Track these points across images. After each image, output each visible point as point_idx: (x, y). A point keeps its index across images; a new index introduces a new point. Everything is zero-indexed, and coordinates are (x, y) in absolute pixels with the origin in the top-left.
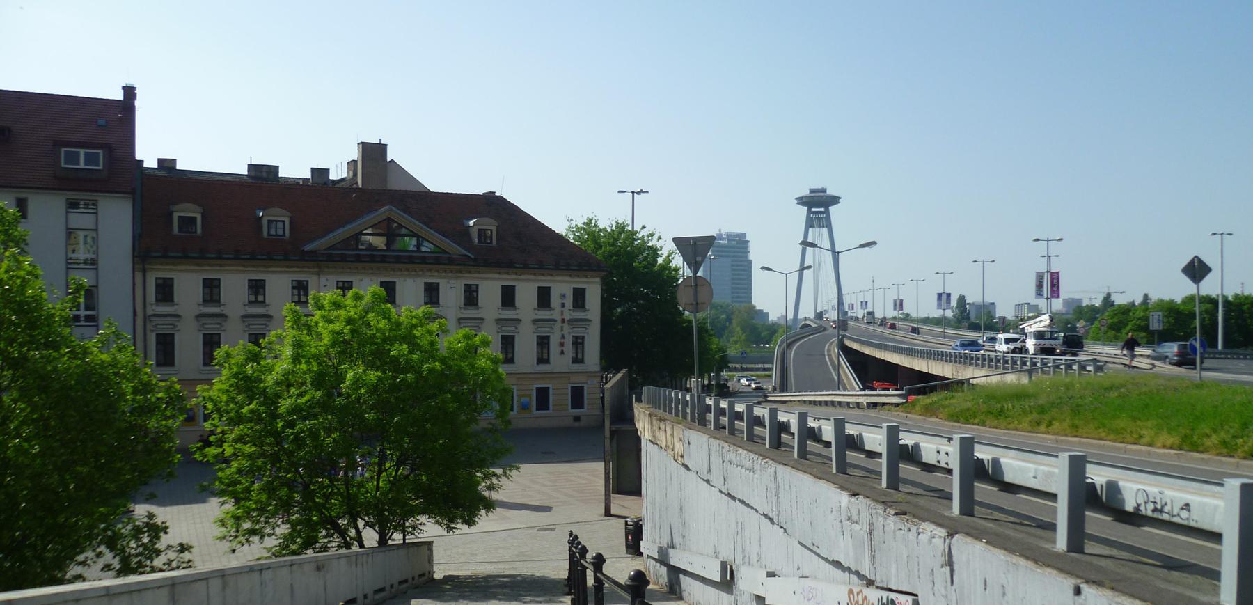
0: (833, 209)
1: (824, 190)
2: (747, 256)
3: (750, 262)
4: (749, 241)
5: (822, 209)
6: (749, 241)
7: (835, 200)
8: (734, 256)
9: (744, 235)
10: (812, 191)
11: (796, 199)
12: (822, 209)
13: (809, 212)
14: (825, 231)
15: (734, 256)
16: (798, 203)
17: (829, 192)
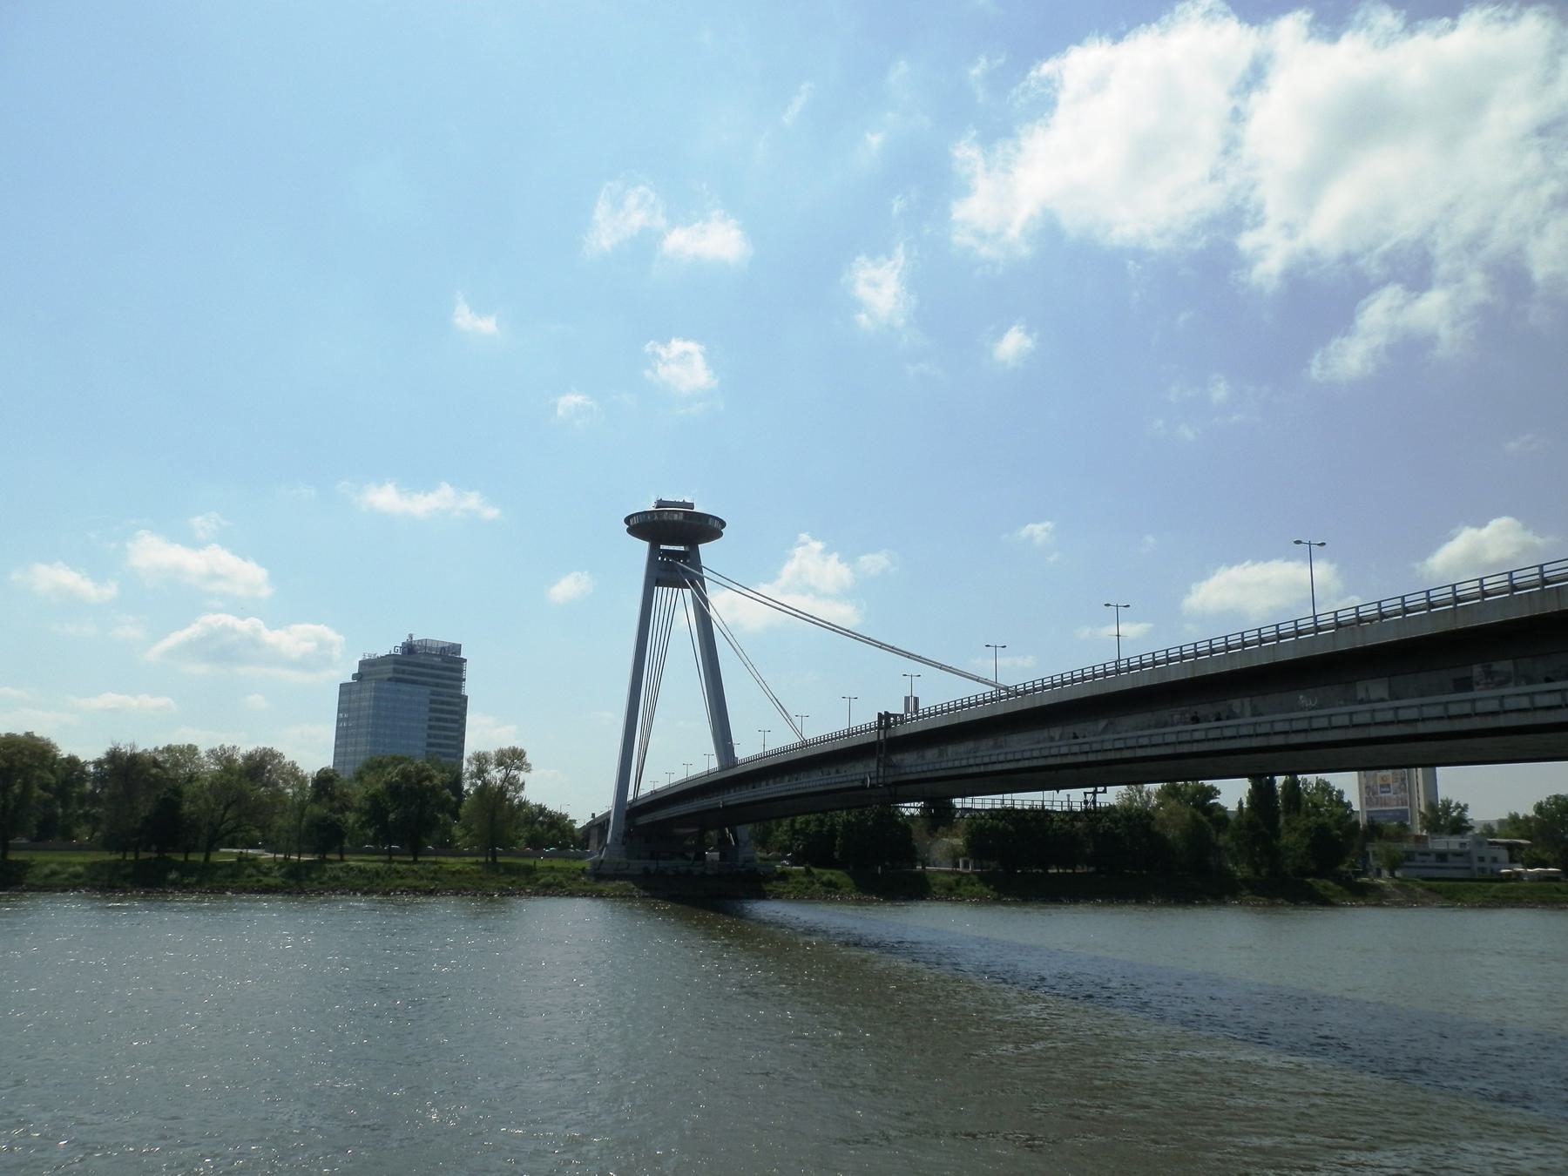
0: (705, 549)
1: (691, 506)
2: (460, 688)
3: (465, 699)
4: (465, 660)
5: (682, 548)
6: (465, 660)
7: (708, 528)
8: (437, 685)
9: (456, 648)
10: (660, 503)
11: (627, 520)
12: (682, 548)
13: (654, 551)
14: (687, 592)
15: (437, 685)
16: (630, 531)
17: (697, 509)
